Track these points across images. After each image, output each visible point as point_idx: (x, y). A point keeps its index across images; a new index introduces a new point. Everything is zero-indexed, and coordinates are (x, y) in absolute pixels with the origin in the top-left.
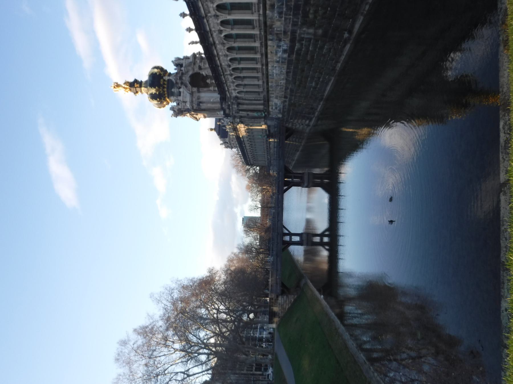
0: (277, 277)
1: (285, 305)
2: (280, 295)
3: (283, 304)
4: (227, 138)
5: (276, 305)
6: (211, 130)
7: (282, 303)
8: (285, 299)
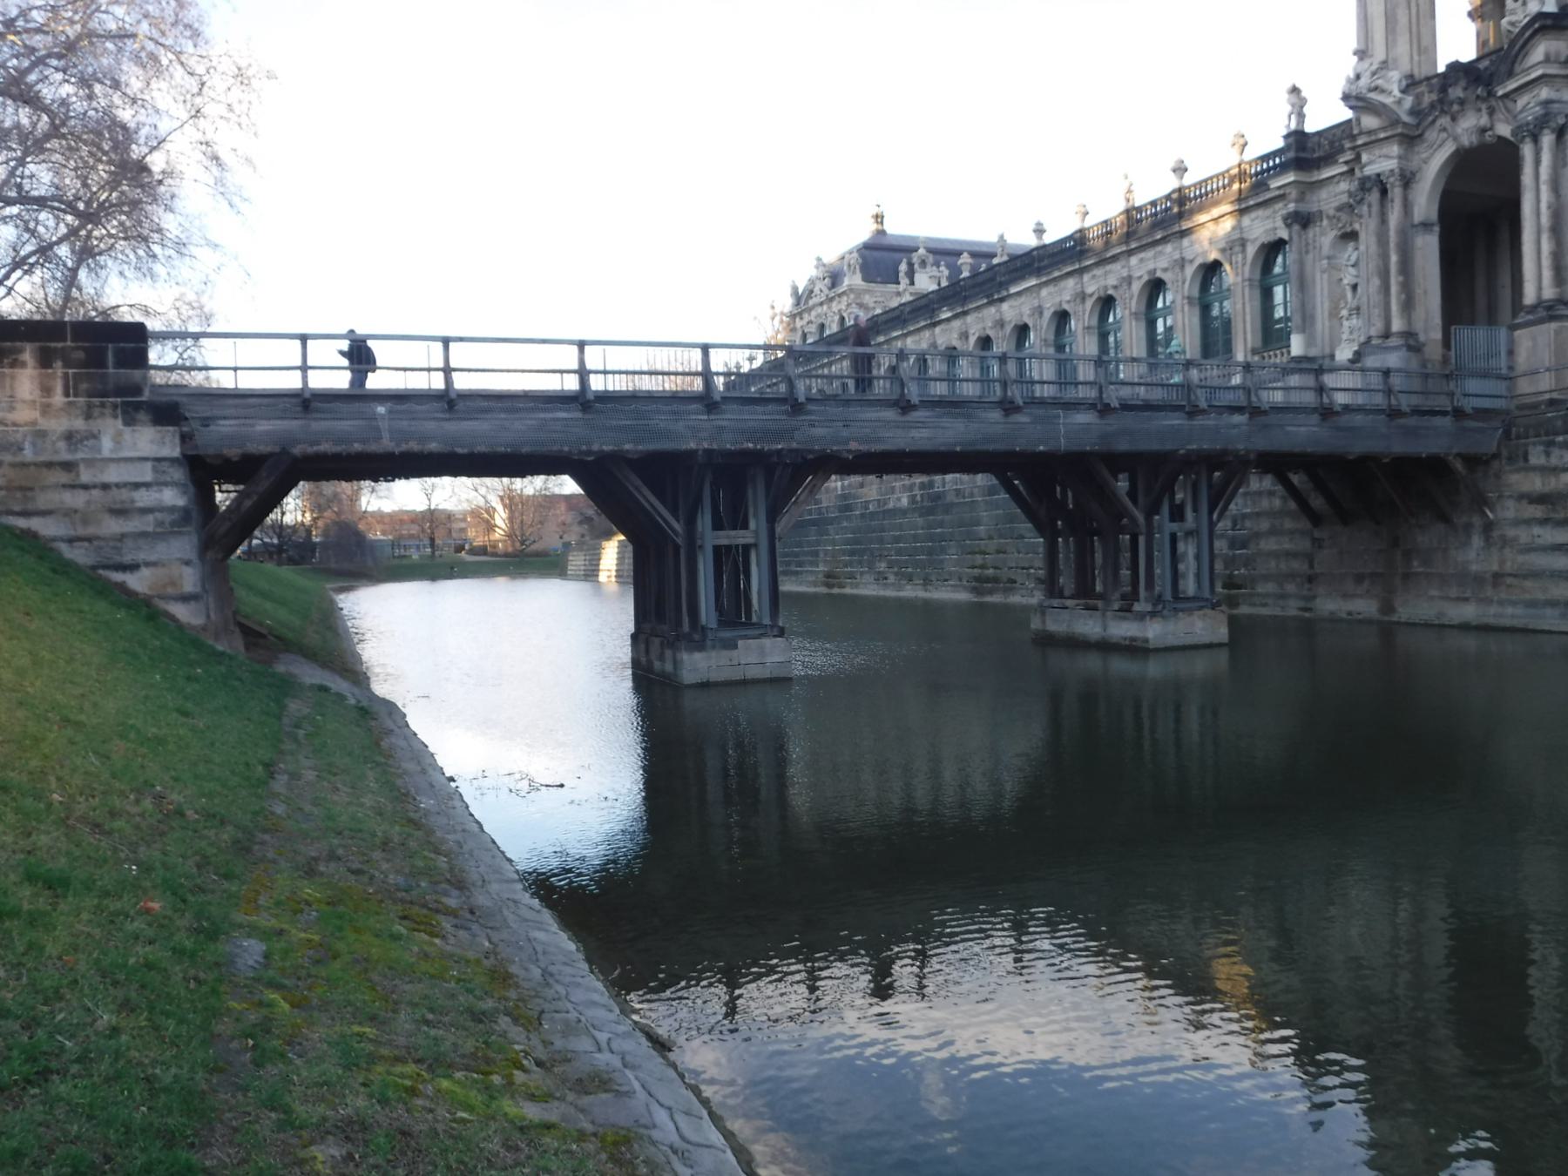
0: (381, 410)
1: (76, 500)
2: (185, 438)
3: (86, 476)
4: (865, 279)
5: (58, 399)
6: (879, 218)
7: (90, 463)
8: (144, 498)
